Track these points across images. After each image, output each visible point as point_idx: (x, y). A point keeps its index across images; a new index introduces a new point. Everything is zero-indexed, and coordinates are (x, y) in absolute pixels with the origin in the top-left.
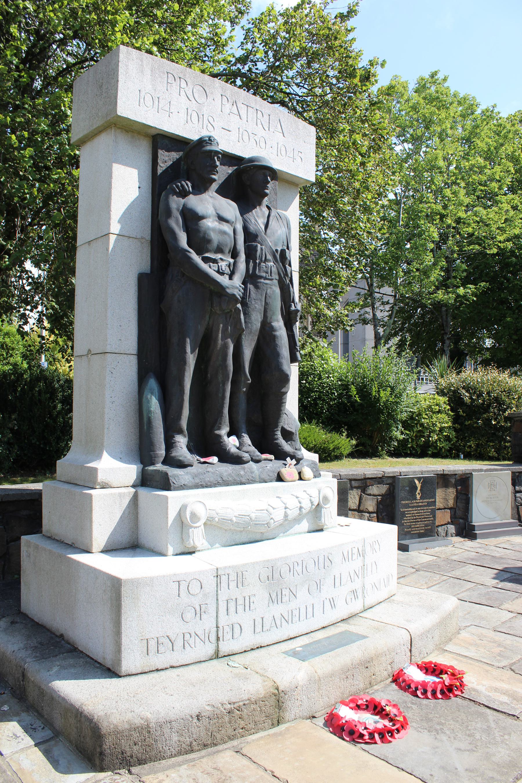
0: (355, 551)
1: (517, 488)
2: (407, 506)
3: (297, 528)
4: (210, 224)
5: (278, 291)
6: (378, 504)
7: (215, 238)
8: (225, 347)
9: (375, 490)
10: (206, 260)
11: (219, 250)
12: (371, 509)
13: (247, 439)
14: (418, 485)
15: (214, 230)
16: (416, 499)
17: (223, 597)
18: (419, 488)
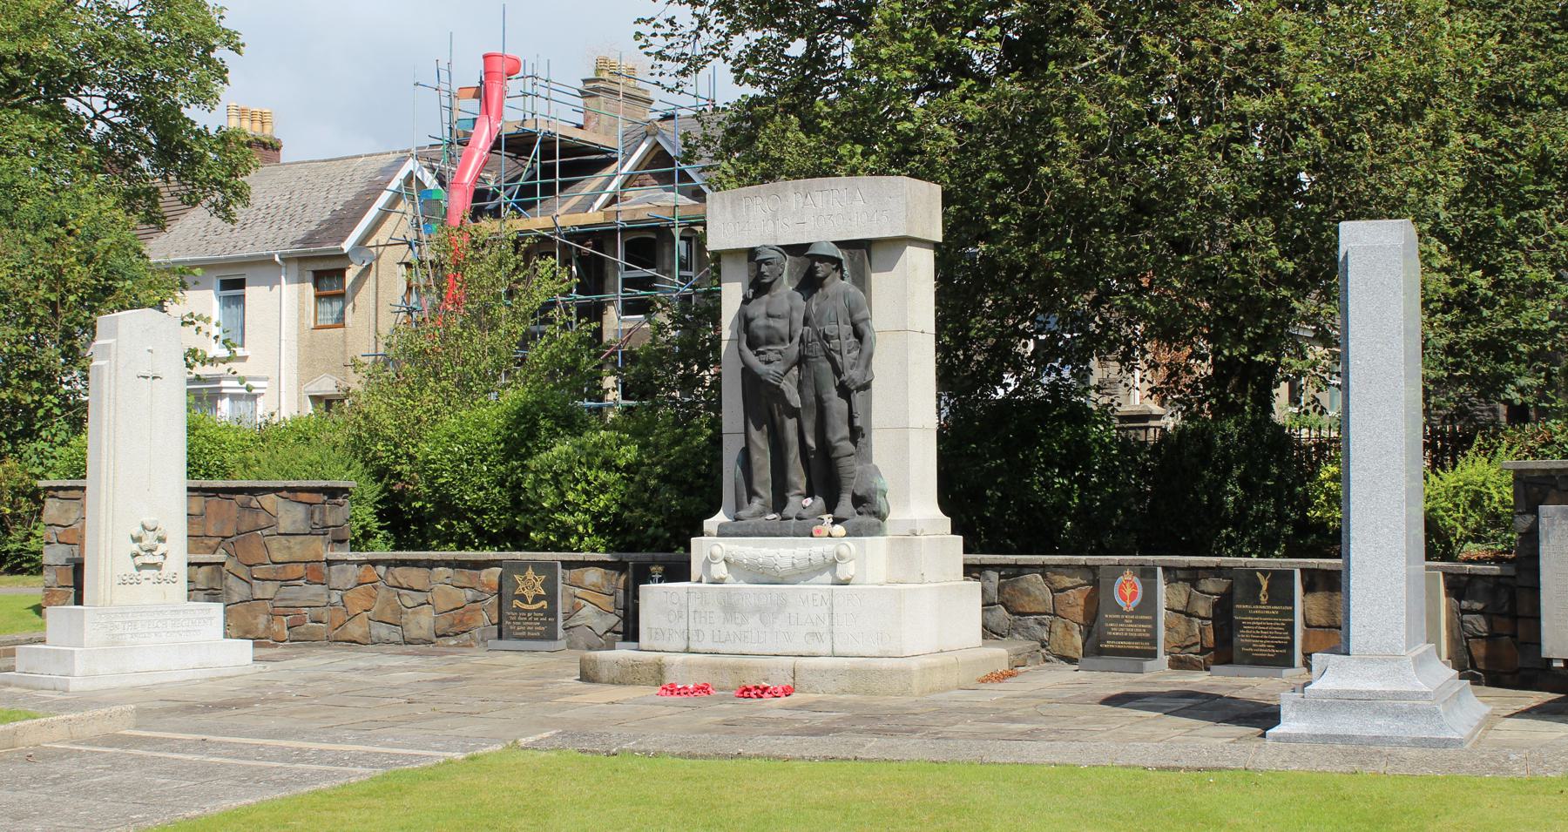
0: (818, 598)
1: (1465, 604)
2: (1244, 613)
3: (818, 578)
4: (760, 322)
5: (827, 365)
6: (1215, 605)
7: (762, 334)
8: (783, 423)
9: (1210, 585)
10: (758, 354)
11: (769, 342)
12: (1202, 613)
13: (820, 501)
14: (1265, 584)
15: (759, 327)
16: (1259, 603)
17: (691, 610)
18: (1265, 587)
